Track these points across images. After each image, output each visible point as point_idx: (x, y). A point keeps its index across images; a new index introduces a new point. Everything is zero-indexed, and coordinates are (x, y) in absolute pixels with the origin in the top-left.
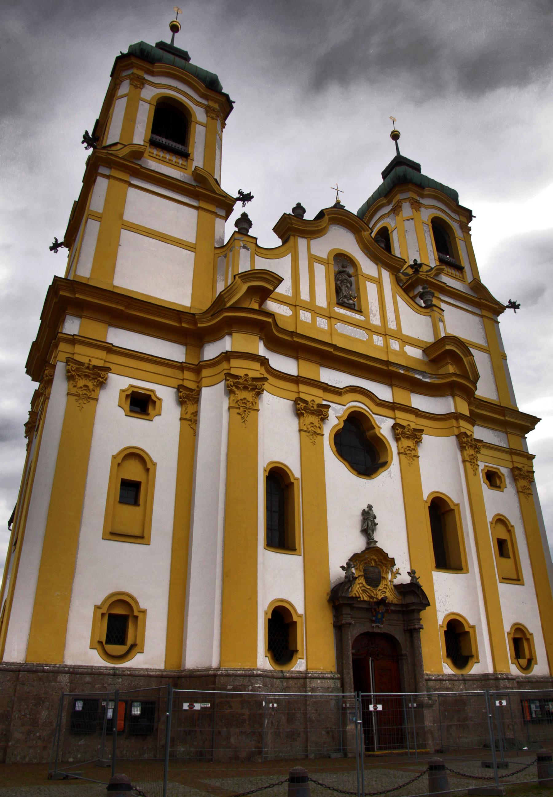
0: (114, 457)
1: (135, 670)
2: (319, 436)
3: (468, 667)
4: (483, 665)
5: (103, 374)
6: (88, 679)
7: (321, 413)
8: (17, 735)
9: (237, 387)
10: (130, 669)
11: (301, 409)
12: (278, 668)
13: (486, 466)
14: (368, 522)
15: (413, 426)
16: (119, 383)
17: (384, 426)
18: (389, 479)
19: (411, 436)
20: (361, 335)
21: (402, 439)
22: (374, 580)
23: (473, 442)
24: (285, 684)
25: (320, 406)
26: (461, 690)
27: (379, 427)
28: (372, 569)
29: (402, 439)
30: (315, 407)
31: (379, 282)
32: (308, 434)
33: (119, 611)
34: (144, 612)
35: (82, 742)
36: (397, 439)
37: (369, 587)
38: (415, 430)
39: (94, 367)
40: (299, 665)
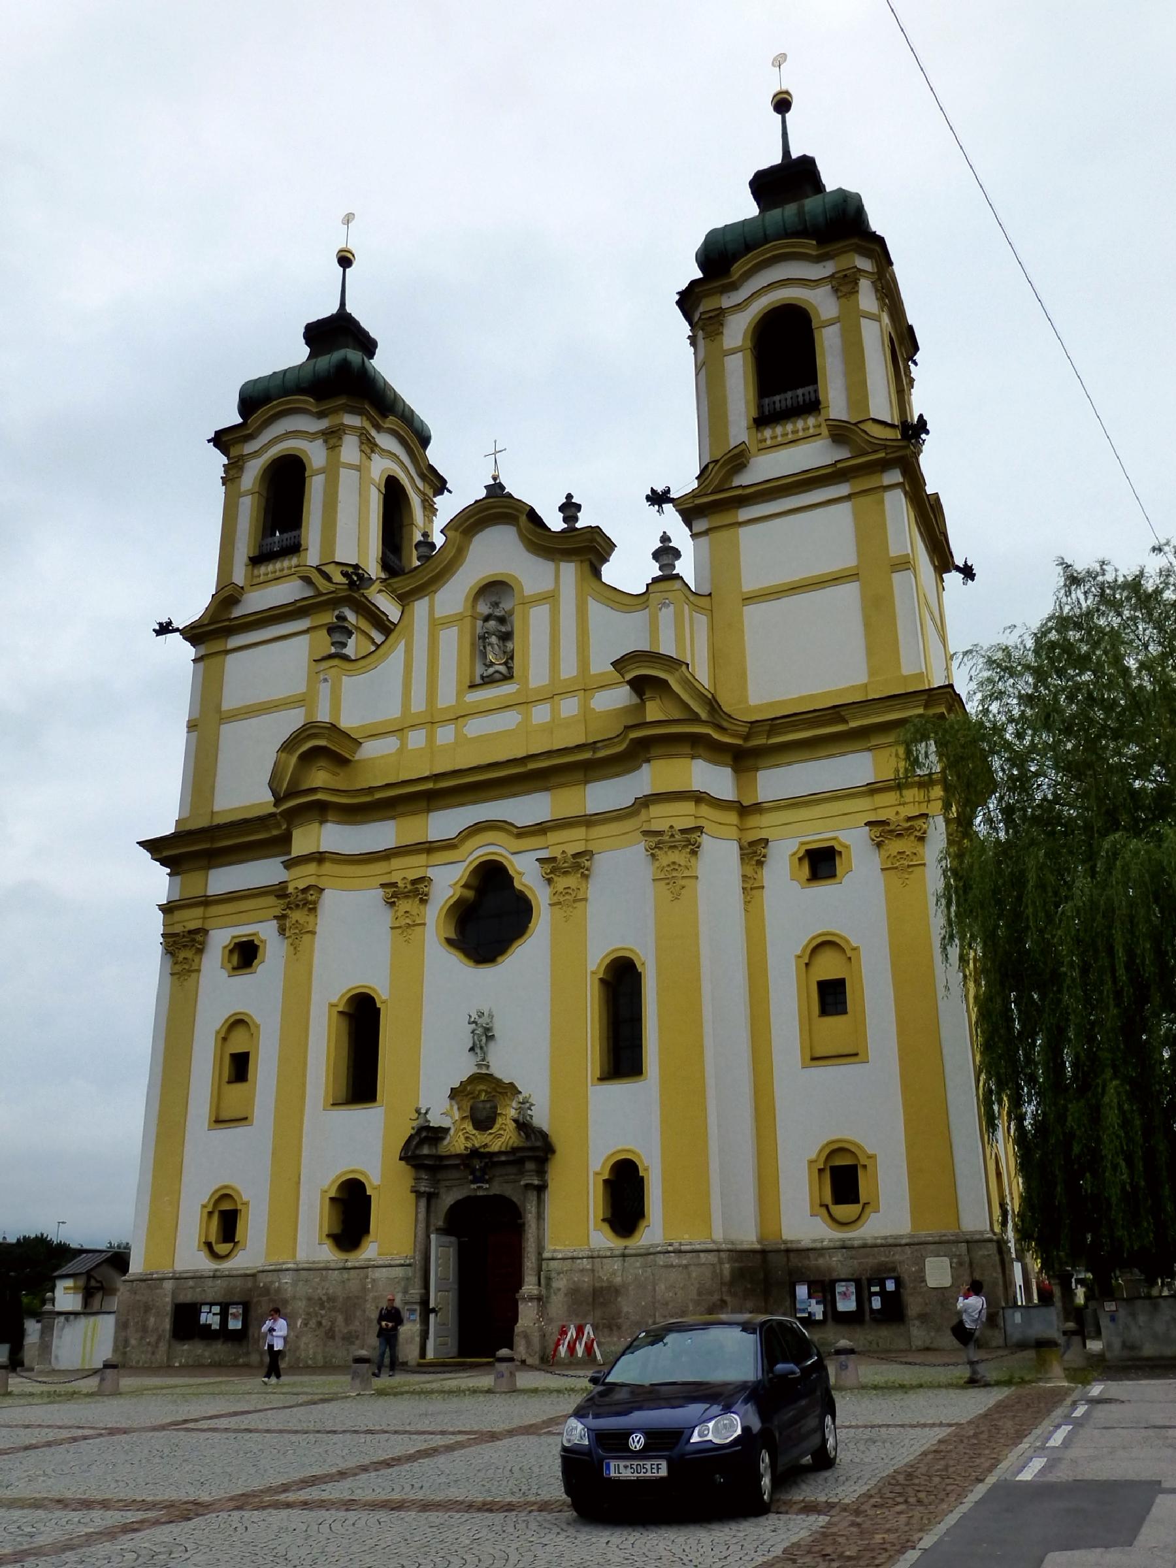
0: (218, 1033)
1: (237, 1269)
2: (416, 928)
3: (637, 1235)
4: (653, 1232)
5: (199, 938)
6: (191, 1283)
7: (418, 890)
8: (133, 1342)
9: (291, 909)
10: (231, 1269)
11: (394, 894)
12: (343, 1256)
13: (803, 844)
14: (483, 1036)
15: (572, 849)
16: (220, 939)
17: (526, 870)
18: (529, 956)
19: (572, 868)
20: (509, 720)
21: (556, 879)
22: (483, 1121)
23: (678, 837)
24: (346, 1276)
25: (414, 882)
26: (613, 1271)
27: (519, 873)
28: (481, 1105)
29: (556, 879)
30: (409, 887)
31: (551, 598)
32: (399, 931)
33: (226, 1206)
34: (246, 1204)
35: (186, 1347)
36: (550, 881)
37: (474, 1132)
38: (575, 856)
39: (190, 932)
40: (369, 1251)
